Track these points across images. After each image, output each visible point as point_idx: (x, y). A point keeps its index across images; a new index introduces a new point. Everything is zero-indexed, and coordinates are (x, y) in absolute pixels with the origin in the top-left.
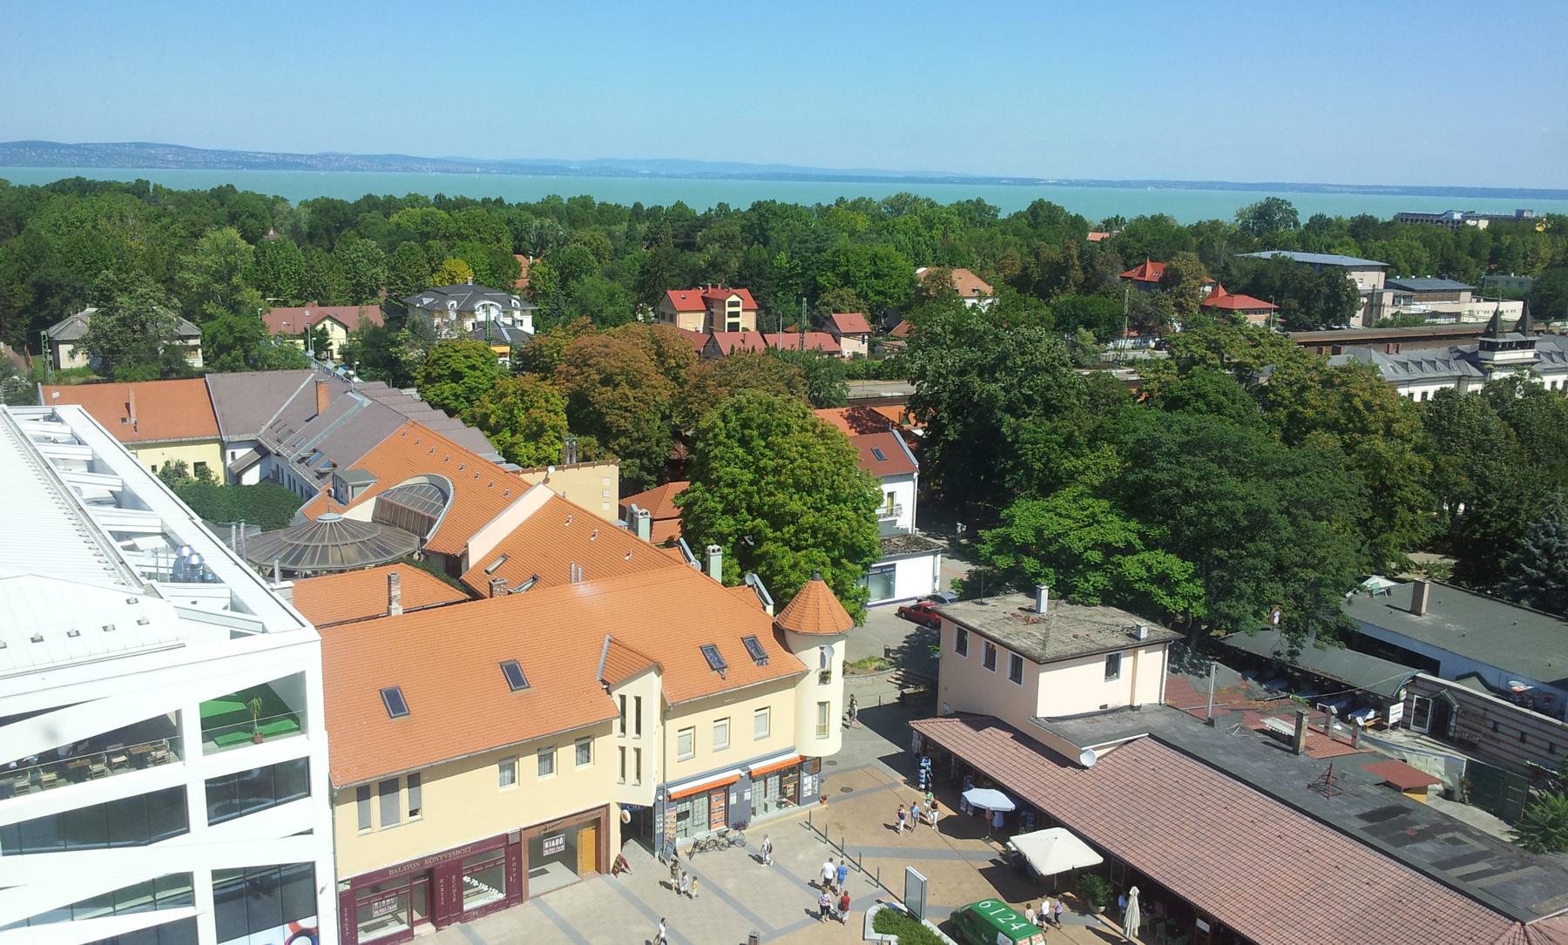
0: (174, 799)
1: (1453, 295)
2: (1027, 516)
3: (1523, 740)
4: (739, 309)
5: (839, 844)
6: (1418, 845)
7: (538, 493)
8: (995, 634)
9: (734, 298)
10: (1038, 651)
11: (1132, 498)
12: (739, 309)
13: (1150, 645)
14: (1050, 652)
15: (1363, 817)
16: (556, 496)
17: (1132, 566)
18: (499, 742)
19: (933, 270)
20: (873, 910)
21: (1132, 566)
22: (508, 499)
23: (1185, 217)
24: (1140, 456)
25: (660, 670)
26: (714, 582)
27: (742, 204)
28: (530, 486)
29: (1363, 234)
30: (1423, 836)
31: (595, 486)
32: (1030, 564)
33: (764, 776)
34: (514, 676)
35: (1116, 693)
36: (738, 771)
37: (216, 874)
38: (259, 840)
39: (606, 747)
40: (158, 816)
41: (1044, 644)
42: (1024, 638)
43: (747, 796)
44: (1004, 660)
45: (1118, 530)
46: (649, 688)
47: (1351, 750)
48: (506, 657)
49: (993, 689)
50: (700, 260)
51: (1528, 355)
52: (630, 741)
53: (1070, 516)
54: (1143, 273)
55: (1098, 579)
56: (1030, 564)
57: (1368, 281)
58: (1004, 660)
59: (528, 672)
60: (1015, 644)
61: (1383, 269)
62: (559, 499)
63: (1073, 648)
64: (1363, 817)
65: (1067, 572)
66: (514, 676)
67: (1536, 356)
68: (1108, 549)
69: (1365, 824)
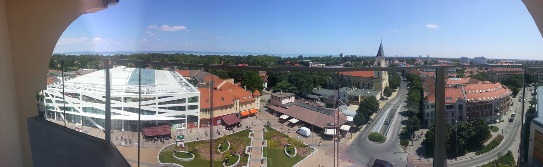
0: (185, 107)
2: (279, 84)
7: (225, 82)
11: (290, 81)
17: (290, 88)
21: (290, 88)
22: (222, 82)
24: (290, 76)
25: (239, 99)
27: (247, 55)
32: (280, 89)
34: (223, 99)
37: (188, 116)
38: (193, 113)
39: (233, 108)
40: (182, 109)
42: (280, 96)
44: (278, 99)
45: (288, 84)
46: (238, 101)
49: (277, 102)
50: (242, 61)
52: (236, 106)
53: (284, 83)
55: (287, 90)
56: (280, 89)
58: (278, 99)
65: (284, 90)
66: (223, 99)
68: (288, 87)
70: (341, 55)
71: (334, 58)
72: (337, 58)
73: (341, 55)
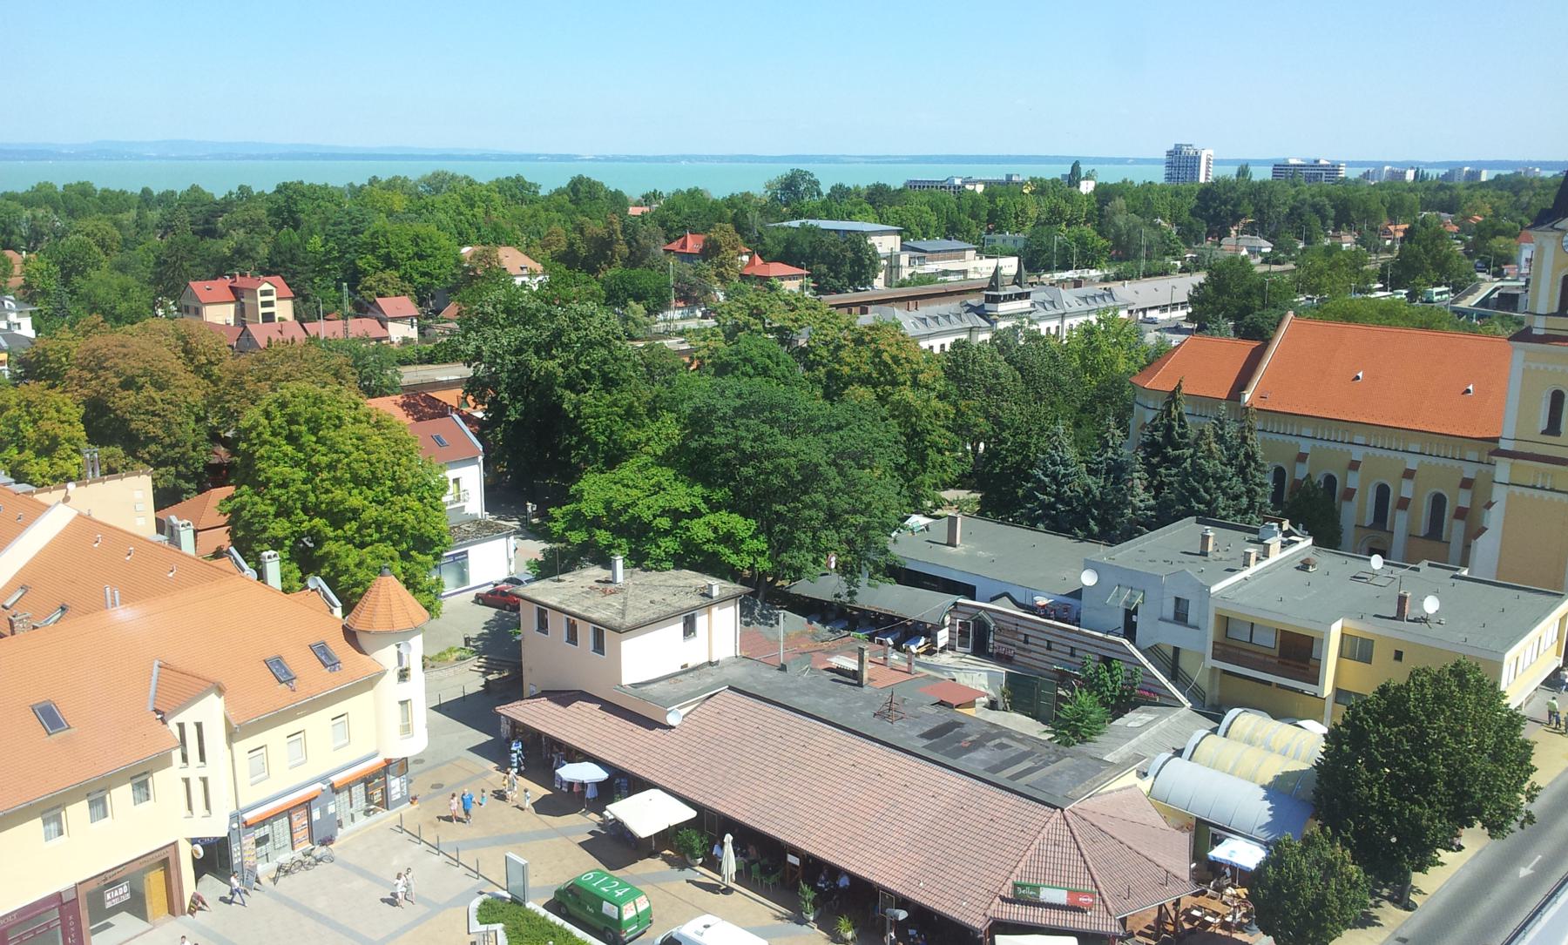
1: (959, 254)
2: (594, 490)
3: (1049, 648)
4: (273, 298)
5: (433, 841)
6: (972, 755)
7: (57, 514)
8: (575, 609)
9: (266, 287)
10: (617, 621)
11: (694, 462)
12: (273, 298)
13: (723, 601)
14: (629, 620)
15: (923, 736)
16: (80, 515)
17: (699, 530)
18: (39, 792)
19: (479, 249)
20: (476, 903)
22: (22, 523)
23: (719, 189)
24: (698, 422)
25: (220, 691)
26: (274, 590)
27: (265, 184)
28: (45, 508)
29: (879, 199)
30: (976, 745)
31: (127, 500)
32: (603, 537)
33: (348, 787)
34: (50, 718)
35: (694, 652)
36: (319, 786)
39: (165, 782)
41: (623, 613)
42: (603, 610)
43: (331, 809)
44: (585, 634)
45: (682, 495)
46: (210, 711)
47: (909, 677)
48: (38, 699)
49: (577, 663)
50: (224, 247)
51: (1024, 305)
52: (194, 770)
53: (639, 486)
54: (684, 246)
55: (669, 544)
56: (603, 537)
57: (886, 244)
58: (585, 634)
59: (65, 711)
60: (595, 616)
61: (899, 233)
62: (85, 525)
63: (650, 614)
64: (923, 736)
65: (638, 539)
66: (50, 718)
67: (1033, 305)
68: (676, 515)
69: (926, 742)
70: (1181, 162)
71: (1105, 194)
72: (1142, 199)
73: (1181, 162)
